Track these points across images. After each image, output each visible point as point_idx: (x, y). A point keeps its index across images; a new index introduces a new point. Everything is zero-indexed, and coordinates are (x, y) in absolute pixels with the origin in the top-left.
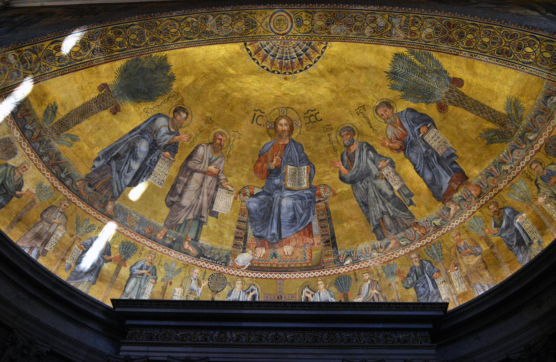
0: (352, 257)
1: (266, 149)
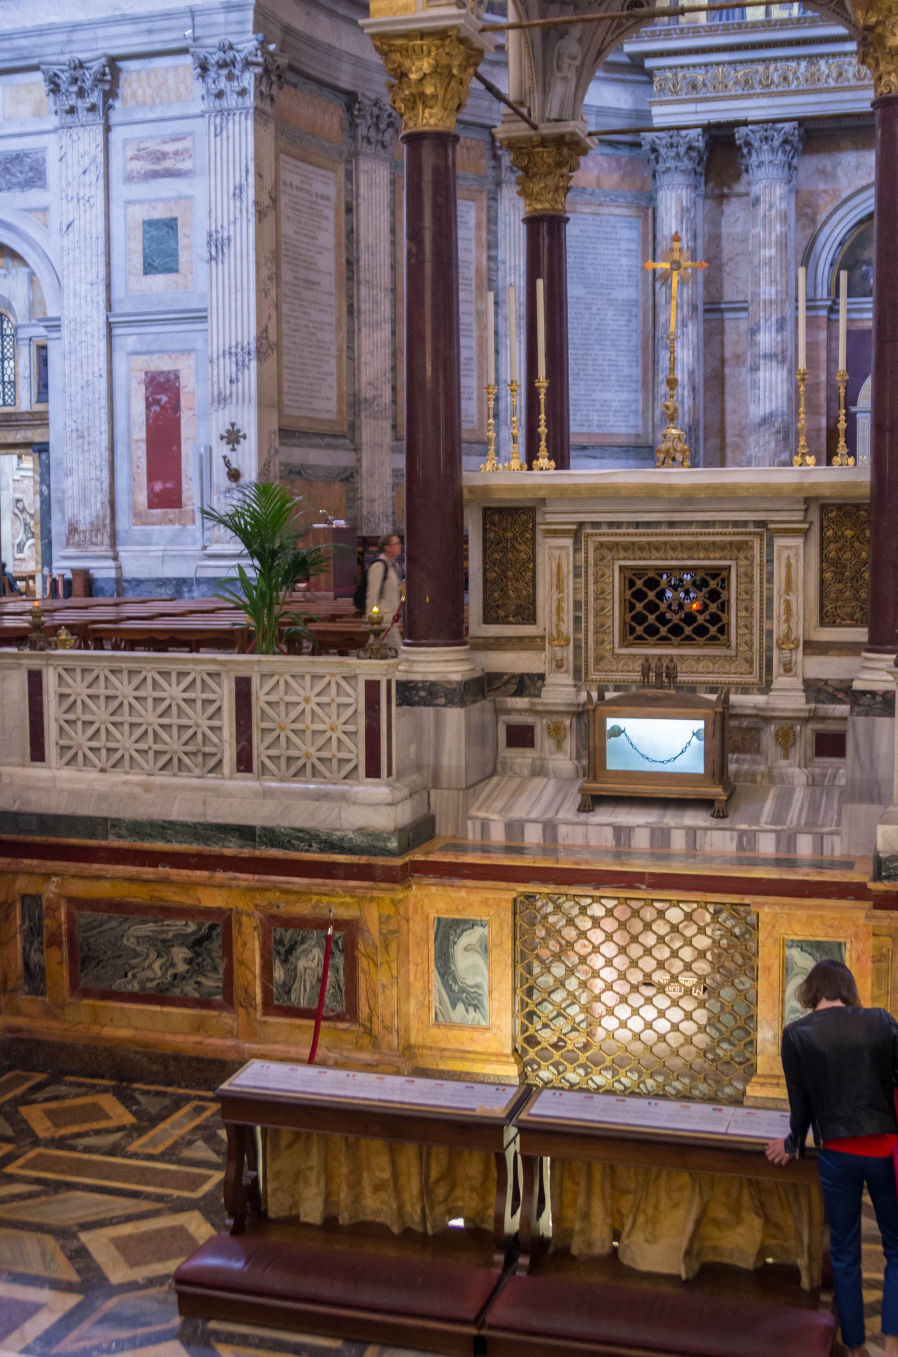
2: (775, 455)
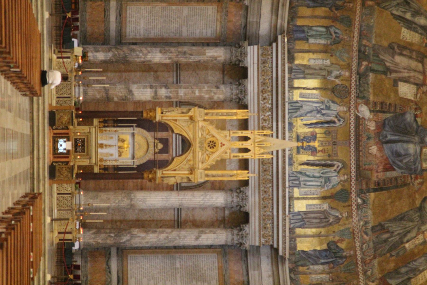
0: (363, 204)
2: (116, 96)
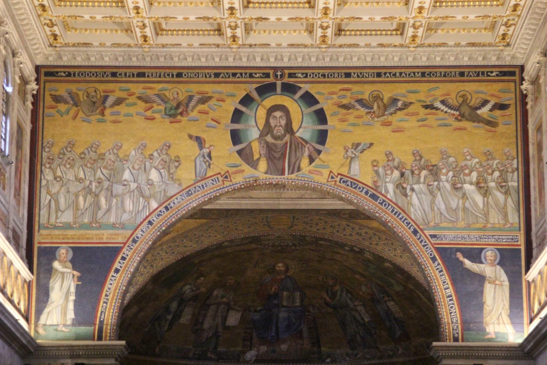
1: (267, 281)
